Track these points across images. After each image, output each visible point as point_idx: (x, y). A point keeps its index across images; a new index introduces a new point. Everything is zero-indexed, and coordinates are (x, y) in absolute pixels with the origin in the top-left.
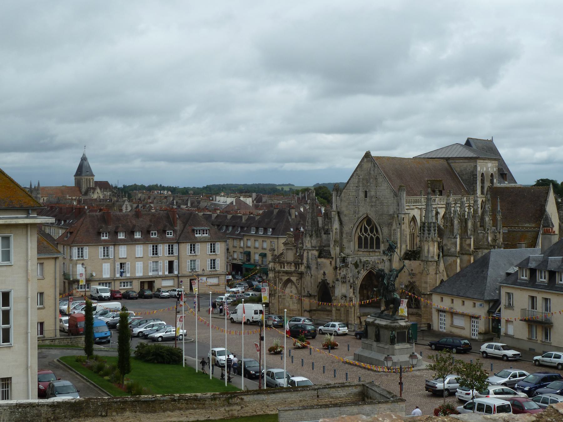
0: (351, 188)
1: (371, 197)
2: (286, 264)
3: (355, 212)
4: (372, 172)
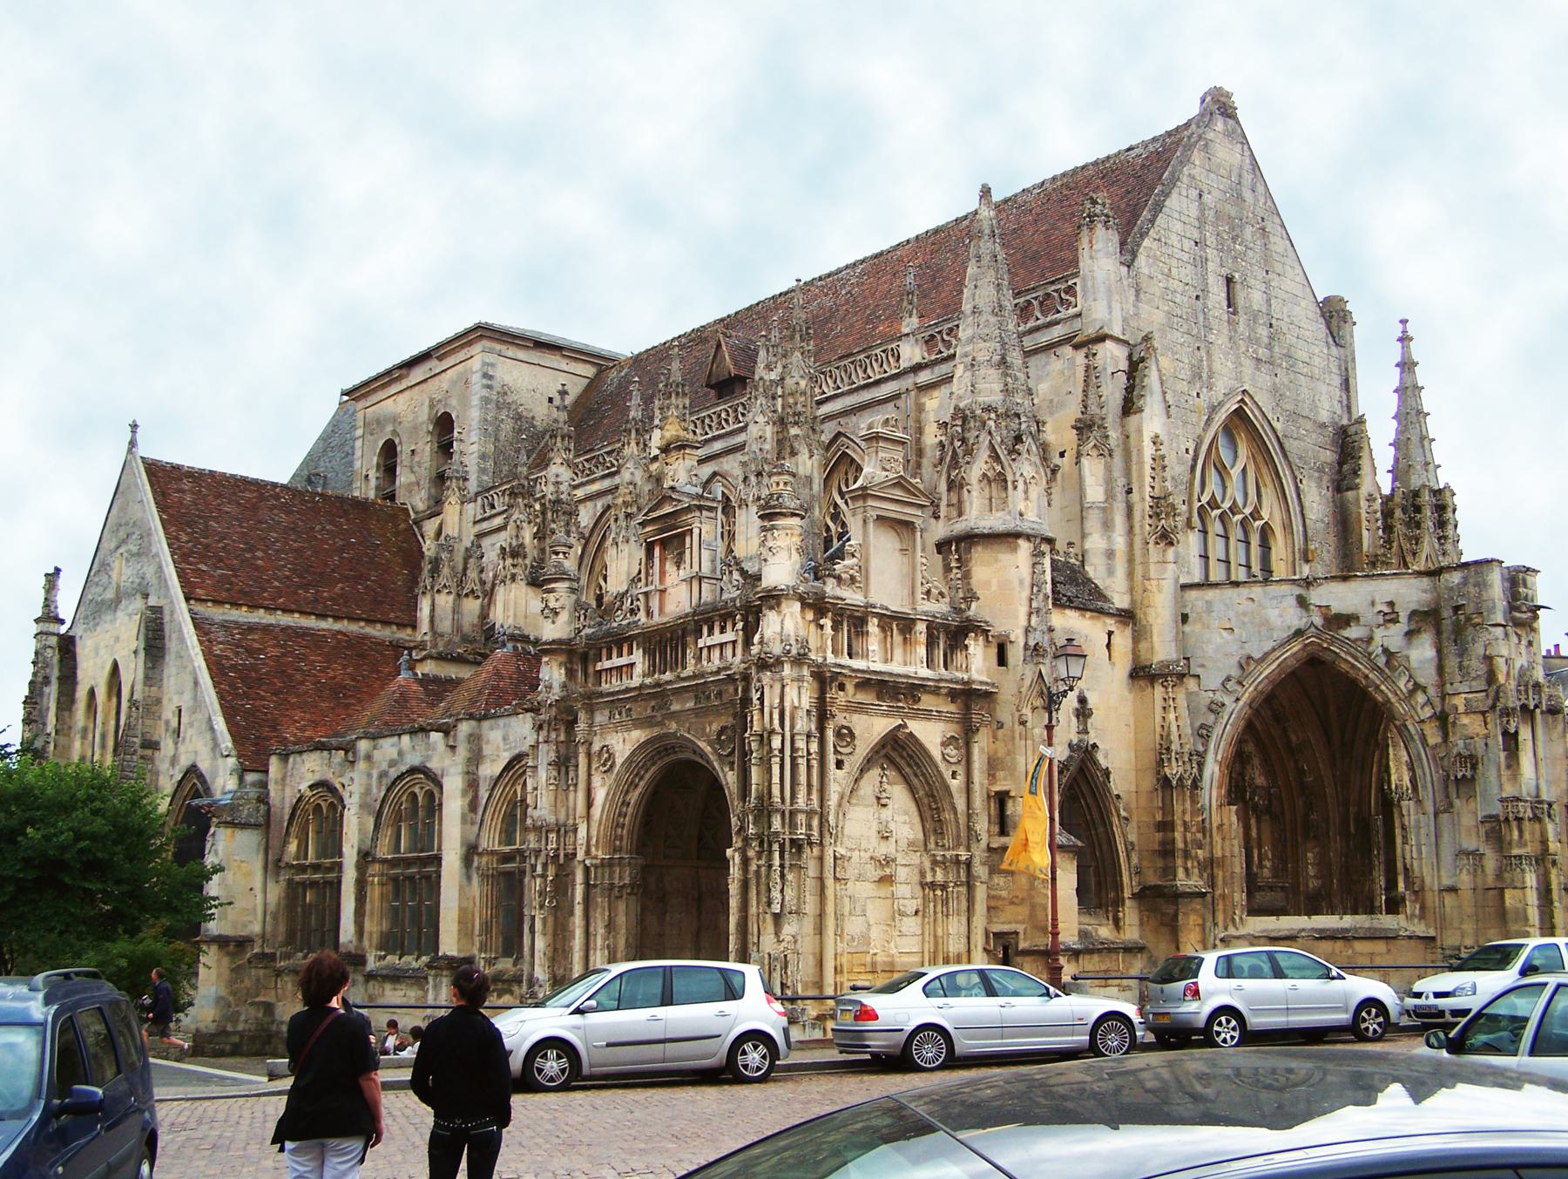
0: (1174, 240)
1: (1254, 317)
2: (873, 626)
3: (1196, 375)
4: (1247, 195)
